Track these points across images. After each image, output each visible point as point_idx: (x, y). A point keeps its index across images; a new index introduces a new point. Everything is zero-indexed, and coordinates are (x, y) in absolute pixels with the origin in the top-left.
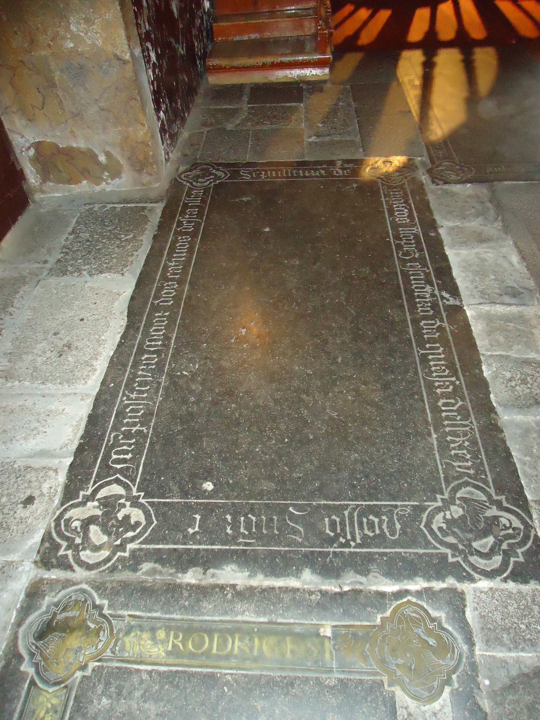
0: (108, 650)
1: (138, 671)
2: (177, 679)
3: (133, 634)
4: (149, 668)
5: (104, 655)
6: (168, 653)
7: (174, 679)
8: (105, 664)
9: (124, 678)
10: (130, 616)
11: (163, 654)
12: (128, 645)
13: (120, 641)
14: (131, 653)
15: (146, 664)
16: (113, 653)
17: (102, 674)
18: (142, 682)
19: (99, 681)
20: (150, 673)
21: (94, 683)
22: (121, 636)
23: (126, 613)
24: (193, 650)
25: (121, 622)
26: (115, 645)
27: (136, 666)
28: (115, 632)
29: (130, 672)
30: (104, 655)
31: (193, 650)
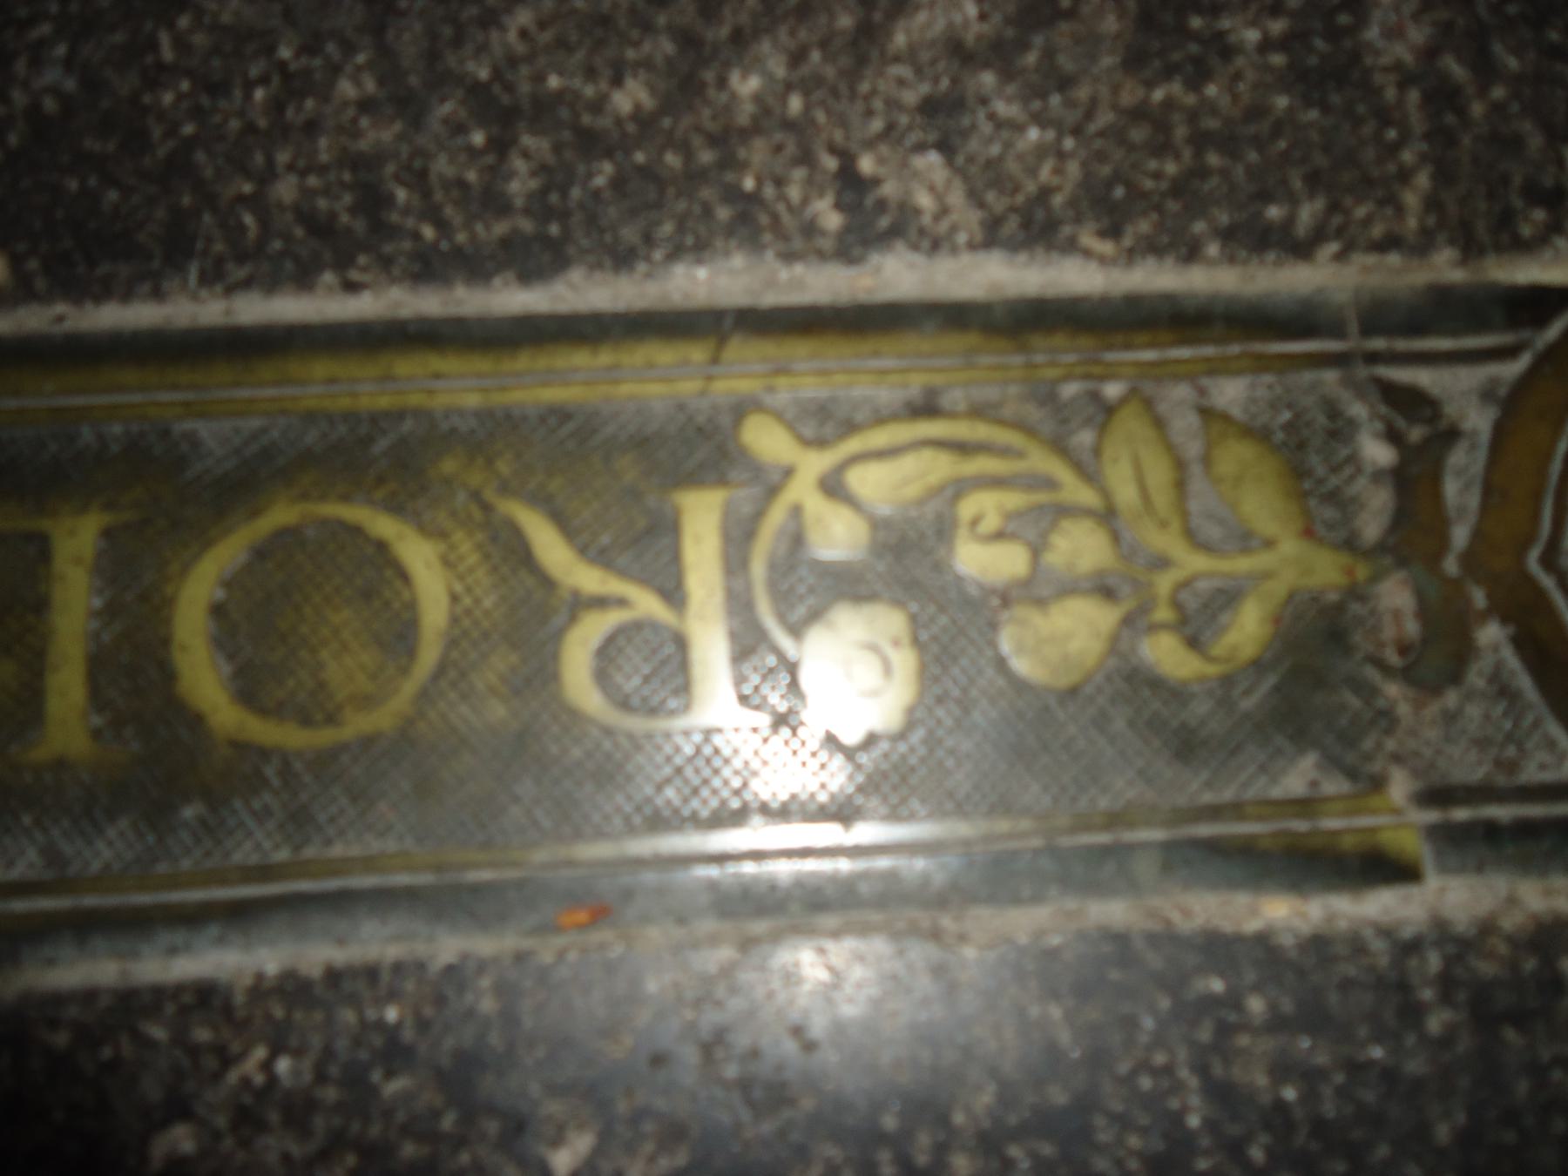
0: (1479, 421)
1: (1036, 229)
2: (520, 184)
3: (1247, 629)
4: (897, 275)
5: (1512, 370)
6: (705, 449)
7: (554, 178)
8: (1445, 267)
9: (1162, 147)
10: (1398, 871)
11: (766, 440)
12: (1262, 504)
13: (1371, 528)
14: (1184, 424)
15: (955, 316)
16: (1408, 403)
17: (1444, 175)
18: (943, 119)
19: (1443, 97)
20: (871, 224)
21: (1485, 70)
22: (1396, 596)
23: (1454, 896)
24: (383, 526)
25: (1468, 767)
26: (1415, 479)
27: (1077, 276)
28: (1491, 634)
29: (1110, 209)
30: (1512, 370)
31: (383, 526)
